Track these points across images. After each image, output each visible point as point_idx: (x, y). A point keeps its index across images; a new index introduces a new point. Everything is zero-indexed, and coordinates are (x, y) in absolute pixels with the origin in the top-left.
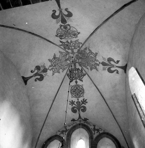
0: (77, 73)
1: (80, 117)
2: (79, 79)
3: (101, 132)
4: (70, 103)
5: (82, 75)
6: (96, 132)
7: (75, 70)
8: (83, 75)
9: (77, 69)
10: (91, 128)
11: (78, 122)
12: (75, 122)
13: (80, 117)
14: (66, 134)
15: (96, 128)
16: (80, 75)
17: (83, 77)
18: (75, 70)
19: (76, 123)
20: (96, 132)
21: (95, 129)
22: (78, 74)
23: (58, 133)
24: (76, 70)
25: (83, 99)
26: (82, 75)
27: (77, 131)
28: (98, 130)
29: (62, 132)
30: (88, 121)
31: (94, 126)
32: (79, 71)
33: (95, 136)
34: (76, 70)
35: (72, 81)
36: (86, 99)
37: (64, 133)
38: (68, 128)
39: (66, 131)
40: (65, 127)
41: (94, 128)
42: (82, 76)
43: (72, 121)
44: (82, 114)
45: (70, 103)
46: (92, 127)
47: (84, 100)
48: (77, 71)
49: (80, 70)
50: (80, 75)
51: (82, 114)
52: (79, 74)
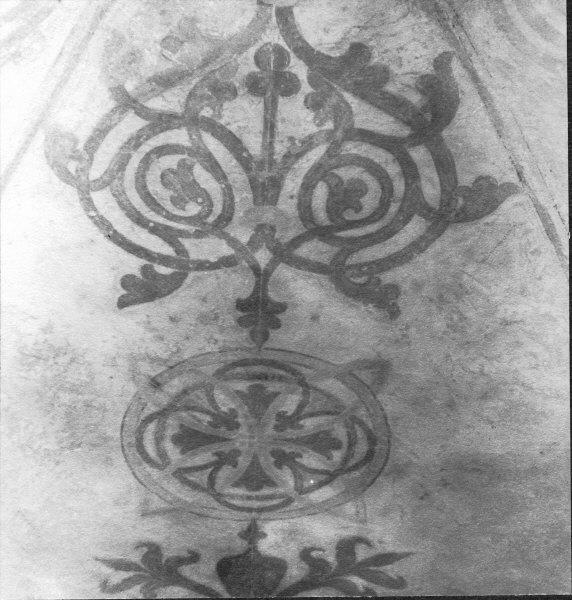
0: (292, 157)
2: (335, 273)
4: (117, 577)
5: (414, 204)
7: (254, 86)
8: (426, 211)
9: (306, 53)
16: (369, 202)
17: (418, 246)
18: (254, 86)
22: (319, 172)
24: (289, 86)
25: (346, 547)
26: (414, 204)
32: (366, 116)
34: (289, 86)
35: (175, 283)
36: (379, 550)
42: (414, 228)
45: (117, 577)
47: (362, 553)
48: (314, 104)
49: (393, 105)
50: (369, 202)
52: (347, 174)
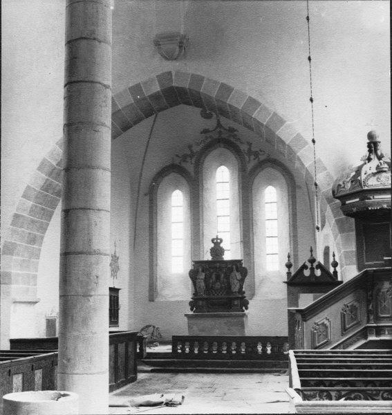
1: (219, 125)
3: (262, 158)
6: (252, 157)
10: (242, 149)
11: (216, 136)
12: (208, 135)
13: (219, 125)
14: (193, 162)
15: (253, 149)
19: (210, 137)
20: (252, 157)
21: (250, 152)
23: (177, 161)
27: (215, 152)
28: (256, 154)
29: (184, 158)
30: (235, 133)
31: (250, 144)
33: (250, 166)
37: (188, 159)
38: (196, 149)
39: (191, 156)
40: (190, 147)
41: (250, 149)
43: (201, 133)
44: (223, 121)
46: (244, 148)
51: (223, 121)
